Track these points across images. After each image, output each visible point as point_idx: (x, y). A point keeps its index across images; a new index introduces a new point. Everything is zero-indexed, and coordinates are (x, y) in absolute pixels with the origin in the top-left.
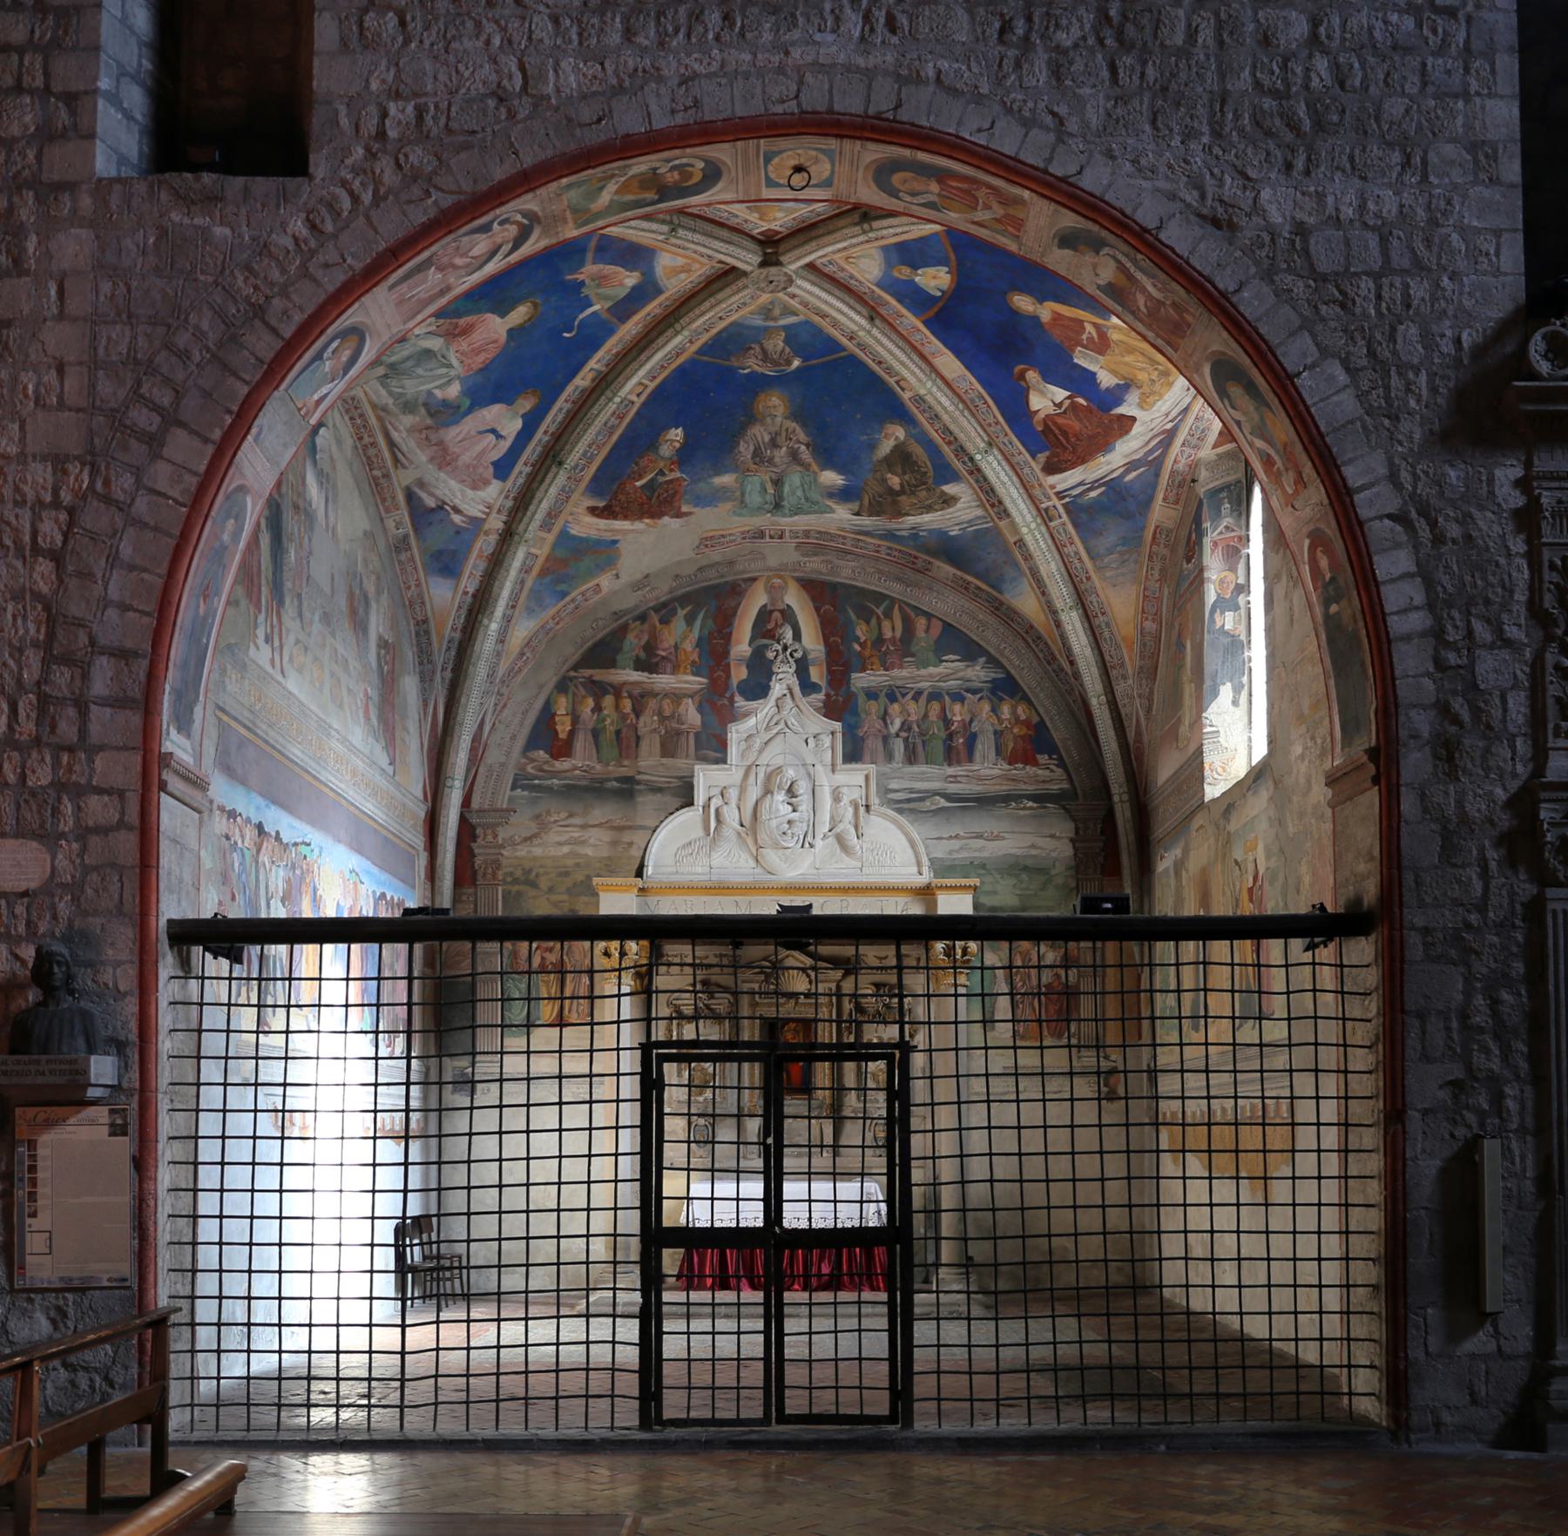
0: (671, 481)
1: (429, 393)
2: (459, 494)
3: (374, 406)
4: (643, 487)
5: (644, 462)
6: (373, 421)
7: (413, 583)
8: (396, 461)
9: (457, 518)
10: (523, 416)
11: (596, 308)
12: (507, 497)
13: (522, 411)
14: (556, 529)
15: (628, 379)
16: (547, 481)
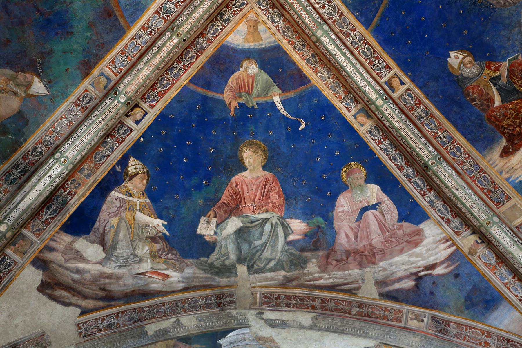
0: (511, 72)
1: (291, 243)
2: (414, 259)
3: (282, 285)
4: (503, 100)
5: (474, 93)
6: (298, 292)
7: (484, 338)
8: (349, 292)
9: (440, 270)
10: (367, 181)
11: (277, 100)
12: (448, 221)
13: (362, 181)
14: (510, 191)
15: (359, 88)
16: (440, 183)
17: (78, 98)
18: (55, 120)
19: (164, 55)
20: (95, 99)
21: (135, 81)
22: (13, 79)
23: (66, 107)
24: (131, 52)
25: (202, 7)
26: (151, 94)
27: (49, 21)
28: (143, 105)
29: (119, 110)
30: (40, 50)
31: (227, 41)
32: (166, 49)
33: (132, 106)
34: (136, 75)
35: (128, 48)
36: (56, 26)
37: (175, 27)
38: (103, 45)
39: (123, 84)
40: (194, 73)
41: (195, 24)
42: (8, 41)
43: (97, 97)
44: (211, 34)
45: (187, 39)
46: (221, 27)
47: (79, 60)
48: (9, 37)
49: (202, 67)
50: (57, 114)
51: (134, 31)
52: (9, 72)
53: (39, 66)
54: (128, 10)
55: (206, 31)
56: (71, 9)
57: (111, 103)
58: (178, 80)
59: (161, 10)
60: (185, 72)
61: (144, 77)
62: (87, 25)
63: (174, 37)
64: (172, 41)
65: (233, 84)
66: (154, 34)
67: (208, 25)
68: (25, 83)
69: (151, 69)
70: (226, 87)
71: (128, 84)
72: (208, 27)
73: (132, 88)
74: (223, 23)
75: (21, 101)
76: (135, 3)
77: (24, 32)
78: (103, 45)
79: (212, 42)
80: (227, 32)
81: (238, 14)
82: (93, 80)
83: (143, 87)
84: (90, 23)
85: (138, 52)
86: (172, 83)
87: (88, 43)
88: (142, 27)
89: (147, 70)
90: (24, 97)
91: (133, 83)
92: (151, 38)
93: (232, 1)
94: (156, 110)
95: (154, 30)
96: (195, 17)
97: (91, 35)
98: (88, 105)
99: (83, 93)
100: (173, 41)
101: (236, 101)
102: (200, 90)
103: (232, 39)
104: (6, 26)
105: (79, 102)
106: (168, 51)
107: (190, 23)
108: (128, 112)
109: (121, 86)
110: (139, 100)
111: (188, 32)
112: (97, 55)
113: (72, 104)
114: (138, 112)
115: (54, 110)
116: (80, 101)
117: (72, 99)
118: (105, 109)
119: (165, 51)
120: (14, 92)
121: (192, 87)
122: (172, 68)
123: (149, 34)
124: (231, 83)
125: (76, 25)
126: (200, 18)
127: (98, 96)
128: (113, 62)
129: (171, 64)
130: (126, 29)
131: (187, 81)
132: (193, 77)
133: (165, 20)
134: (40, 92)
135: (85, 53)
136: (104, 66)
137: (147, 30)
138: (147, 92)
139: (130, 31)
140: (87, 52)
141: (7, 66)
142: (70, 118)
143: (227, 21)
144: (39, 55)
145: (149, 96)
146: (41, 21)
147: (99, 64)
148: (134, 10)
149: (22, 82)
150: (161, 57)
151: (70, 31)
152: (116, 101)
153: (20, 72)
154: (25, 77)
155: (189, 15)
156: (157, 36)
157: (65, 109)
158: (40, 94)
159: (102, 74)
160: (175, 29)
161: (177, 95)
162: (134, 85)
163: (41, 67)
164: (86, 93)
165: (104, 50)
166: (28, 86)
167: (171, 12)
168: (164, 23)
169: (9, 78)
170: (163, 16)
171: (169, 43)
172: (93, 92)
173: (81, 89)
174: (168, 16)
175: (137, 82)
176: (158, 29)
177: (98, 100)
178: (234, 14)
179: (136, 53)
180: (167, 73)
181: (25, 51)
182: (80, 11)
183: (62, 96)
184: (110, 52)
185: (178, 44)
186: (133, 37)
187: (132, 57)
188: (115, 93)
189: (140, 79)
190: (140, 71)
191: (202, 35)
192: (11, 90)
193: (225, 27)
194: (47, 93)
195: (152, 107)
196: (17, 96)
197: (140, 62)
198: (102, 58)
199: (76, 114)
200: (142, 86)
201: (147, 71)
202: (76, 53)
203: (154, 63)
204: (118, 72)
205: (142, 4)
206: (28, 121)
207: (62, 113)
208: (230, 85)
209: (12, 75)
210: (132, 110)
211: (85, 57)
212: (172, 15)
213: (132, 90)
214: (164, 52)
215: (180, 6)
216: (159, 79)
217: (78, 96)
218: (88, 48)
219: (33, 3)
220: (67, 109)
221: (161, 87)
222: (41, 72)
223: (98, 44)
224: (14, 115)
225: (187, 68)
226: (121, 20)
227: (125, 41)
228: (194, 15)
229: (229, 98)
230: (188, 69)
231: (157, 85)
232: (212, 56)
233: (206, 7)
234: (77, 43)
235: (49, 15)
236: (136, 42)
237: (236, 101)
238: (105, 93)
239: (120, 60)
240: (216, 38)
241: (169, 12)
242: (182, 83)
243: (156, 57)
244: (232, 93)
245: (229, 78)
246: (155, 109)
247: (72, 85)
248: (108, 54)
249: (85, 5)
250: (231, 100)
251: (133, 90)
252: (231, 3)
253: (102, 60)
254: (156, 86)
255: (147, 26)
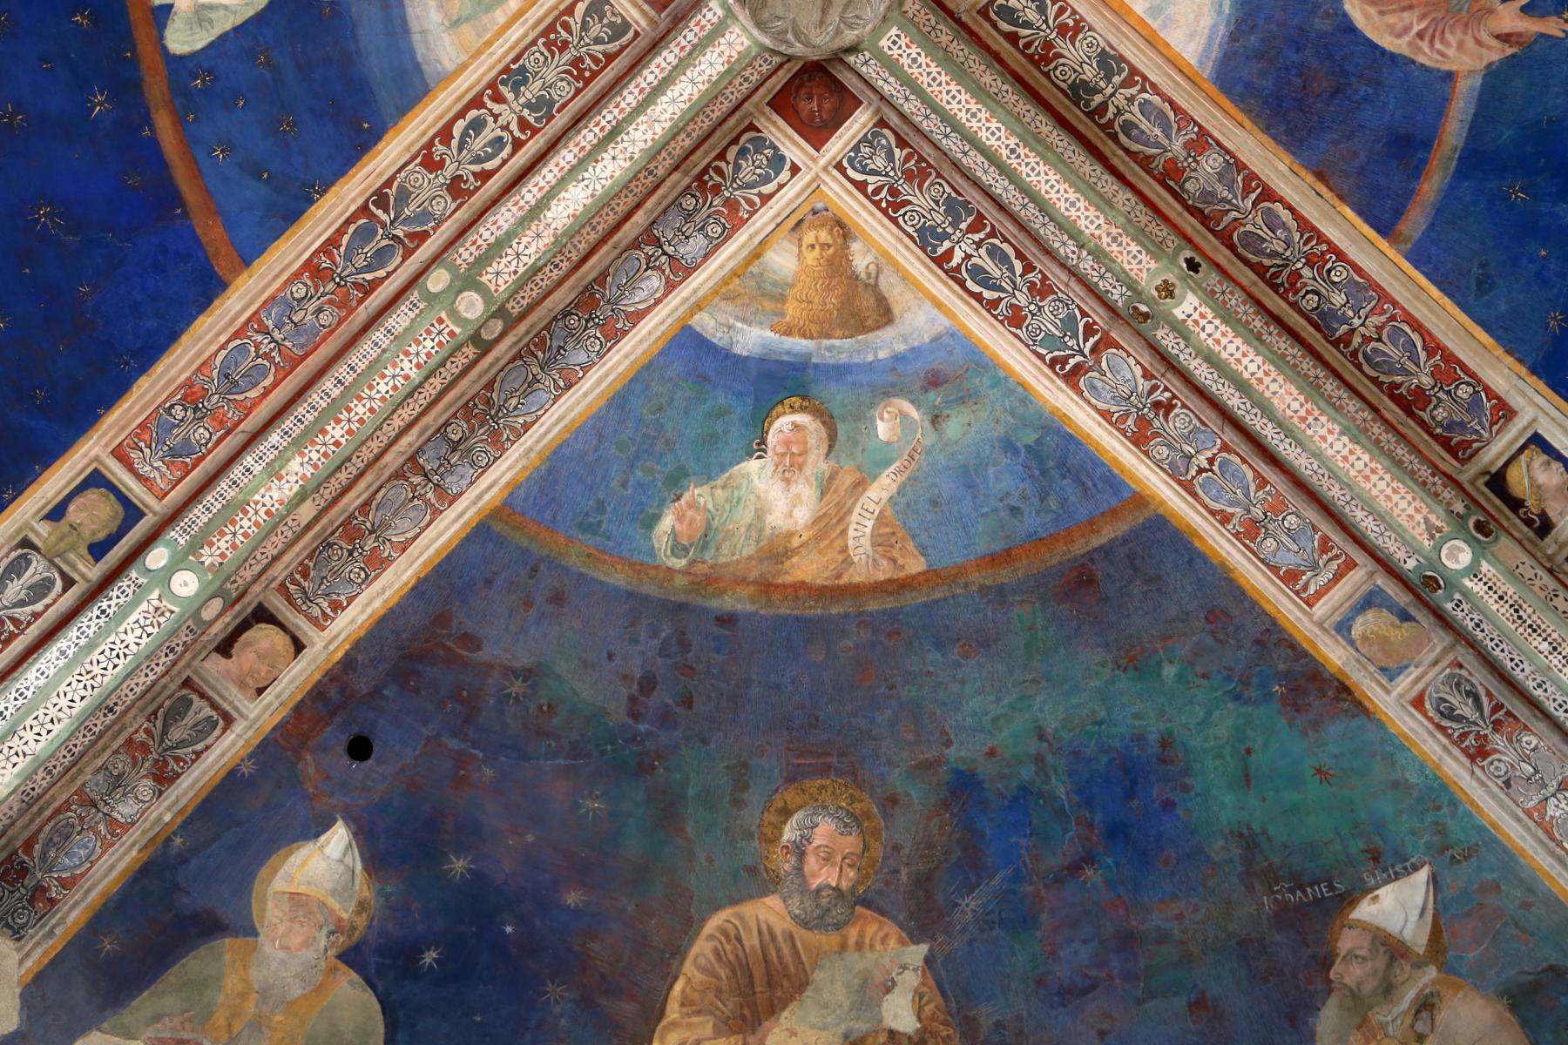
17: (1454, 743)
18: (1552, 853)
19: (1259, 360)
20: (1461, 666)
21: (1375, 492)
22: (1359, 1007)
23: (1494, 796)
24: (1247, 495)
25: (1044, 188)
26: (1441, 414)
27: (1116, 832)
28: (1495, 451)
29: (1513, 574)
30: (1235, 879)
31: (1201, 63)
32: (1231, 348)
33: (1498, 502)
34: (1346, 486)
35: (1230, 510)
36: (1134, 804)
37: (1135, 308)
38: (1214, 616)
39: (1390, 545)
40: (1349, 212)
41: (1122, 220)
42: (1199, 1004)
43: (1451, 657)
44: (1169, 137)
45: (1188, 254)
46: (1133, 91)
47: (1282, 722)
48: (1184, 998)
49: (1320, 176)
50: (1522, 837)
51: (1153, 478)
52: (1328, 1020)
53: (1304, 892)
54: (1064, 502)
55: (1153, 157)
56: (1066, 736)
57: (1475, 608)
58: (1377, 288)
59: (1064, 361)
60: (1341, 256)
61: (1359, 452)
62: (1131, 673)
63: (1179, 313)
64: (1196, 322)
65: (1407, 29)
66: (1168, 395)
67: (1127, 151)
68: (1381, 962)
69: (1323, 419)
70: (1421, 59)
71: (1390, 527)
72: (1135, 147)
73: (1411, 511)
74: (1117, 80)
75: (1458, 988)
76: (1037, 473)
77: (1163, 938)
78: (1214, 616)
79: (1203, 133)
80: (1159, 60)
81: (1074, 12)
82: (1372, 669)
83: (1407, 458)
84: (1123, 662)
85: (1246, 468)
86: (1393, 318)
87: (1204, 676)
88: (1136, 444)
89: (1324, 438)
90: (1439, 969)
91: (1384, 505)
92: (1184, 406)
93: (1021, 43)
94: (1522, 393)
95: (1150, 393)
96: (1088, 219)
97: (1171, 662)
98: (1485, 700)
99: (1430, 719)
100: (1196, 316)
101: (1491, 11)
102: (1432, 185)
103: (1192, 35)
104: (1140, 1002)
105: (1472, 736)
106: (1238, 341)
107: (1114, 239)
108: (1529, 522)
109: (1401, 555)
110: (1472, 469)
111: (1156, 250)
112: (1258, 642)
113: (1478, 771)
114: (1531, 478)
115: (1506, 851)
116: (1464, 736)
117: (1455, 768)
118: (1505, 636)
119: (1238, 355)
120: (1418, 1012)
121: (1415, 222)
122: (1322, 315)
123: (1166, 416)
124: (1399, 36)
125: (1129, 721)
126: (1091, 195)
127: (1445, 651)
128: (1291, 577)
129: (1302, 321)
130: (1147, 514)
131: (1383, 244)
132: (1367, 221)
133: (1107, 343)
134: (1419, 899)
135: (1251, 693)
136: (1310, 616)
137: (1150, 423)
138: (1430, 434)
139: (1153, 497)
140: (1246, 683)
141: (1306, 1023)
142: (1545, 786)
143: (1108, 62)
144: (1258, 887)
145: (1451, 426)
146: (1117, 865)
147: (1297, 636)
148: (1064, 477)
149: (1376, 972)
150: (1266, 374)
151: (1153, 749)
152: (1467, 583)
153: (1332, 975)
154: (1352, 956)
155: (1081, 247)
156: (1174, 380)
157: (1502, 806)
158: (1431, 904)
159: (1343, 628)
160: (1144, 308)
161: (1450, 296)
162: (1396, 498)
163: (1311, 885)
164: (1428, 705)
165: (1235, 612)
166: (1391, 948)
167: (1072, 317)
168: (1118, 346)
169: (1357, 1020)
170: (1086, 351)
171: (1203, 336)
172: (1425, 673)
173: (1411, 723)
174: (1089, 330)
175: (1382, 485)
176: (1147, 375)
177: (1464, 654)
178: (1077, 29)
179: (1250, 475)
180: (1346, 340)
181: (1242, 943)
182: (1075, 701)
183: (1438, 808)
184: (1247, 587)
185: (1209, 296)
186: (1180, 483)
187: (1268, 493)
188: (1431, 583)
189: (1367, 472)
190: (1329, 469)
191: (1170, 176)
192: (1408, 1022)
193: (1134, 71)
194: (1423, 875)
195: (1505, 412)
196: (1435, 1000)
197: (1291, 464)
198: (1274, 622)
199: (1526, 759)
200: (1399, 463)
201: (1330, 439)
202: (1249, 732)
203: (1295, 405)
204: (1337, 557)
205: (1039, 441)
206: (1551, 968)
207: (1519, 820)
208: (1410, 44)
209: (1341, 1007)
210: (1515, 504)
211: (1268, 696)
212: (1084, 314)
213: (1417, 510)
214: (1245, 361)
215: (1045, 278)
216: (1374, 374)
217: (1444, 740)
218: (1229, 679)
219: (1046, 886)
220: (1502, 795)
221: (1411, 366)
222: (1331, 888)
223: (1212, 633)
224: (1525, 1023)
225: (1324, 247)
226: (1108, 533)
227: (1198, 519)
228: (1082, 223)
229: (1479, 43)
230: (1329, 242)
231: (1398, 386)
232: (1267, 129)
233: (1042, 168)
234: (1205, 722)
235: (1091, 826)
236: (1201, 471)
237: (1491, 11)
238: (1432, 619)
239: (1279, 543)
240: (1185, 113)
241: (1069, 324)
242: (1394, 270)
243: (1267, 394)
244: (1452, 28)
245: (1375, 46)
246: (1515, 401)
247: (1393, 764)
248: (1255, 596)
249: (1049, 680)
250: (1484, 37)
251: (1417, 504)
252: (1028, 45)
253: (1282, 622)
254: (1403, 390)
255: (1130, 422)
